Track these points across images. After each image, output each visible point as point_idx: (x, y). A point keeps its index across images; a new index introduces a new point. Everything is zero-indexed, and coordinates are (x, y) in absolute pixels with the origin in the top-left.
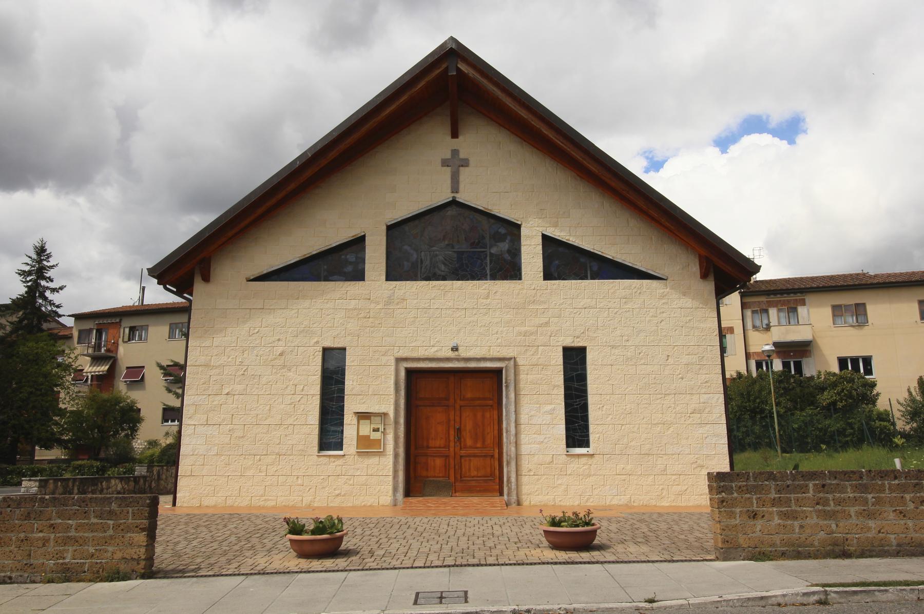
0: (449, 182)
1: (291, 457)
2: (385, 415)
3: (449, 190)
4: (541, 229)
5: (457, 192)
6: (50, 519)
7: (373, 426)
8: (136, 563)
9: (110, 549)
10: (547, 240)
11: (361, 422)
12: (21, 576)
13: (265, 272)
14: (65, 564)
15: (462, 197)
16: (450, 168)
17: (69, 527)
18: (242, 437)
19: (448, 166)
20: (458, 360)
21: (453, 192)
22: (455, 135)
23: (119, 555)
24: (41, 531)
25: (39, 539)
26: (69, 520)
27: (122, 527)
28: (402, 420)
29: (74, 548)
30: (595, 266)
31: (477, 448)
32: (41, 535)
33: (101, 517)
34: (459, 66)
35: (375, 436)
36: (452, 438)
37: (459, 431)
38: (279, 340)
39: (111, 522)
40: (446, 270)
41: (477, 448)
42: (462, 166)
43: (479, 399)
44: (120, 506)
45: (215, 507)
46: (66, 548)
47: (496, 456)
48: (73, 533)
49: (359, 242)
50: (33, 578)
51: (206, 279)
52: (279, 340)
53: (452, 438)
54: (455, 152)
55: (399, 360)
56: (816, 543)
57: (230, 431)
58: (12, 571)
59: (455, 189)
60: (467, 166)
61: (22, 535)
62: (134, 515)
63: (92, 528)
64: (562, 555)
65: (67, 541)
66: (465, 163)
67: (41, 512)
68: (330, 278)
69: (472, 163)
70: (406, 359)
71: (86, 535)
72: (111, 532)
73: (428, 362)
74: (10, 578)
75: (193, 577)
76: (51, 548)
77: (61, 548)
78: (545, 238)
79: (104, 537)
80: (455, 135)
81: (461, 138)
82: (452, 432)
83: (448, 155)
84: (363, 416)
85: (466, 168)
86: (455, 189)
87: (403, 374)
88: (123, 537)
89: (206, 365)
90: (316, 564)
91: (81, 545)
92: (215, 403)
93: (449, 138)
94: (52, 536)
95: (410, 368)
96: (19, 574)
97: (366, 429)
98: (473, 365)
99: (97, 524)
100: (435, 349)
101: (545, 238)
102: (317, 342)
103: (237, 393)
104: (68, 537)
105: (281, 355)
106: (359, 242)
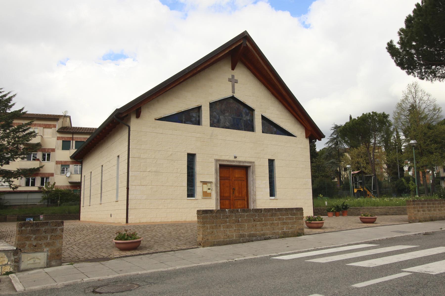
0: (231, 88)
1: (177, 200)
2: (211, 182)
3: (231, 92)
4: (261, 113)
5: (234, 93)
6: (278, 216)
7: (208, 187)
8: (302, 230)
9: (295, 226)
10: (263, 118)
11: (204, 185)
12: (273, 236)
13: (163, 117)
14: (284, 231)
15: (236, 96)
16: (231, 82)
17: (283, 219)
18: (157, 191)
19: (231, 81)
20: (237, 161)
21: (233, 93)
22: (233, 69)
23: (297, 228)
24: (276, 220)
25: (276, 223)
26: (284, 216)
27: (298, 218)
28: (219, 185)
29: (286, 226)
30: (275, 129)
31: (239, 197)
32: (276, 222)
33: (291, 215)
34: (247, 43)
35: (209, 191)
36: (231, 193)
37: (234, 189)
38: (170, 148)
39: (294, 217)
40: (229, 125)
41: (239, 197)
42: (236, 82)
43: (240, 177)
44: (296, 211)
45: (171, 222)
46: (284, 226)
47: (246, 200)
48: (285, 221)
49: (199, 108)
50: (276, 237)
51: (138, 116)
52: (170, 148)
53: (231, 193)
54: (233, 76)
55: (217, 160)
56: (428, 218)
57: (151, 188)
58: (270, 235)
59: (233, 92)
60: (237, 83)
61: (271, 222)
62: (300, 214)
63: (290, 219)
64: (124, 253)
65: (284, 223)
66: (236, 82)
67: (275, 213)
68: (186, 123)
69: (239, 82)
70: (219, 160)
71: (288, 221)
72: (295, 220)
73: (226, 162)
74: (270, 237)
75: (147, 254)
76: (280, 226)
77: (282, 226)
78: (262, 116)
79: (293, 222)
80: (233, 69)
81: (235, 70)
82: (231, 191)
83: (231, 77)
84: (204, 183)
85: (237, 84)
86: (233, 92)
87: (218, 166)
88: (298, 222)
89: (139, 158)
90: (129, 253)
91: (288, 225)
92: (144, 175)
93: (230, 69)
94: (279, 222)
95: (221, 164)
96: (272, 236)
97: (205, 188)
98: (242, 164)
99: (291, 217)
100: (228, 157)
101: (262, 116)
102: (185, 151)
103: (153, 171)
104: (284, 222)
105: (171, 155)
106: (199, 108)
